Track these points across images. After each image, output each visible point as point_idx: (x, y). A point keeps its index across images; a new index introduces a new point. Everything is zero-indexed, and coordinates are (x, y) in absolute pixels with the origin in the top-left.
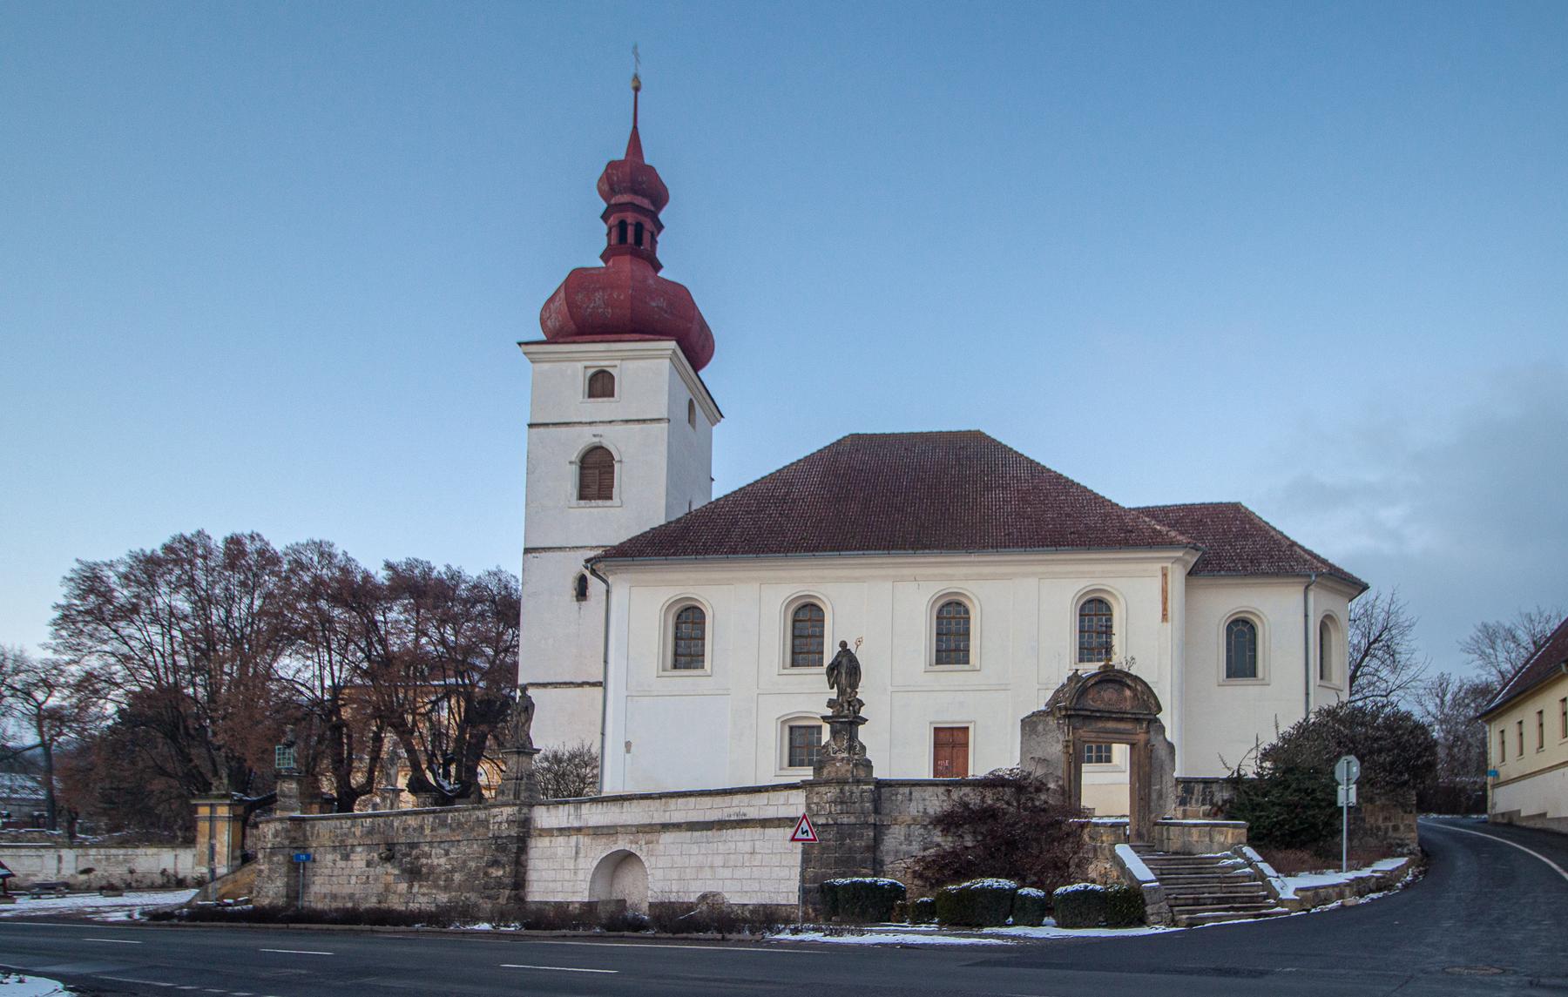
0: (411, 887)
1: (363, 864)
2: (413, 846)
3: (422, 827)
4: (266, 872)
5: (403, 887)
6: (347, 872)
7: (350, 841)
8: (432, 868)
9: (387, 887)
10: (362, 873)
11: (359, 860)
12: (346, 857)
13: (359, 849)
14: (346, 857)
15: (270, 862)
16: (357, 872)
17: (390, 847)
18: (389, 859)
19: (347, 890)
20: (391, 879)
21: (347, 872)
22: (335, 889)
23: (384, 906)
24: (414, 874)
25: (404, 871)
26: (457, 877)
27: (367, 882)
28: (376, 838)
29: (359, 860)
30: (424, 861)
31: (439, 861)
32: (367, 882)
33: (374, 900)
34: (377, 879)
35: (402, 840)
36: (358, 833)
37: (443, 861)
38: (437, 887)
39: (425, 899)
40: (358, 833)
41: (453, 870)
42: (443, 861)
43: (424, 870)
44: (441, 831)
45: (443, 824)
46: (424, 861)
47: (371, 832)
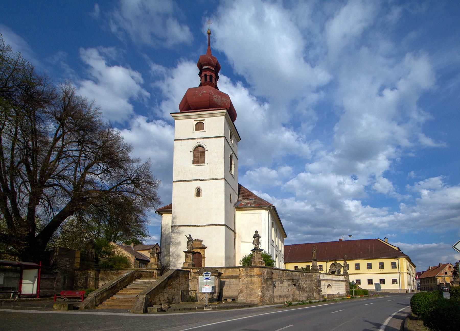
0: (299, 292)
1: (287, 285)
3: (299, 275)
5: (298, 292)
6: (283, 288)
7: (283, 278)
8: (303, 287)
10: (287, 288)
11: (286, 283)
12: (282, 283)
13: (285, 281)
14: (282, 283)
15: (267, 283)
17: (293, 280)
19: (284, 294)
22: (280, 294)
24: (300, 288)
27: (288, 291)
28: (289, 278)
29: (286, 283)
31: (303, 285)
32: (288, 291)
33: (292, 296)
34: (291, 290)
36: (285, 275)
37: (304, 285)
39: (303, 295)
40: (285, 275)
42: (304, 285)
44: (304, 277)
47: (288, 275)
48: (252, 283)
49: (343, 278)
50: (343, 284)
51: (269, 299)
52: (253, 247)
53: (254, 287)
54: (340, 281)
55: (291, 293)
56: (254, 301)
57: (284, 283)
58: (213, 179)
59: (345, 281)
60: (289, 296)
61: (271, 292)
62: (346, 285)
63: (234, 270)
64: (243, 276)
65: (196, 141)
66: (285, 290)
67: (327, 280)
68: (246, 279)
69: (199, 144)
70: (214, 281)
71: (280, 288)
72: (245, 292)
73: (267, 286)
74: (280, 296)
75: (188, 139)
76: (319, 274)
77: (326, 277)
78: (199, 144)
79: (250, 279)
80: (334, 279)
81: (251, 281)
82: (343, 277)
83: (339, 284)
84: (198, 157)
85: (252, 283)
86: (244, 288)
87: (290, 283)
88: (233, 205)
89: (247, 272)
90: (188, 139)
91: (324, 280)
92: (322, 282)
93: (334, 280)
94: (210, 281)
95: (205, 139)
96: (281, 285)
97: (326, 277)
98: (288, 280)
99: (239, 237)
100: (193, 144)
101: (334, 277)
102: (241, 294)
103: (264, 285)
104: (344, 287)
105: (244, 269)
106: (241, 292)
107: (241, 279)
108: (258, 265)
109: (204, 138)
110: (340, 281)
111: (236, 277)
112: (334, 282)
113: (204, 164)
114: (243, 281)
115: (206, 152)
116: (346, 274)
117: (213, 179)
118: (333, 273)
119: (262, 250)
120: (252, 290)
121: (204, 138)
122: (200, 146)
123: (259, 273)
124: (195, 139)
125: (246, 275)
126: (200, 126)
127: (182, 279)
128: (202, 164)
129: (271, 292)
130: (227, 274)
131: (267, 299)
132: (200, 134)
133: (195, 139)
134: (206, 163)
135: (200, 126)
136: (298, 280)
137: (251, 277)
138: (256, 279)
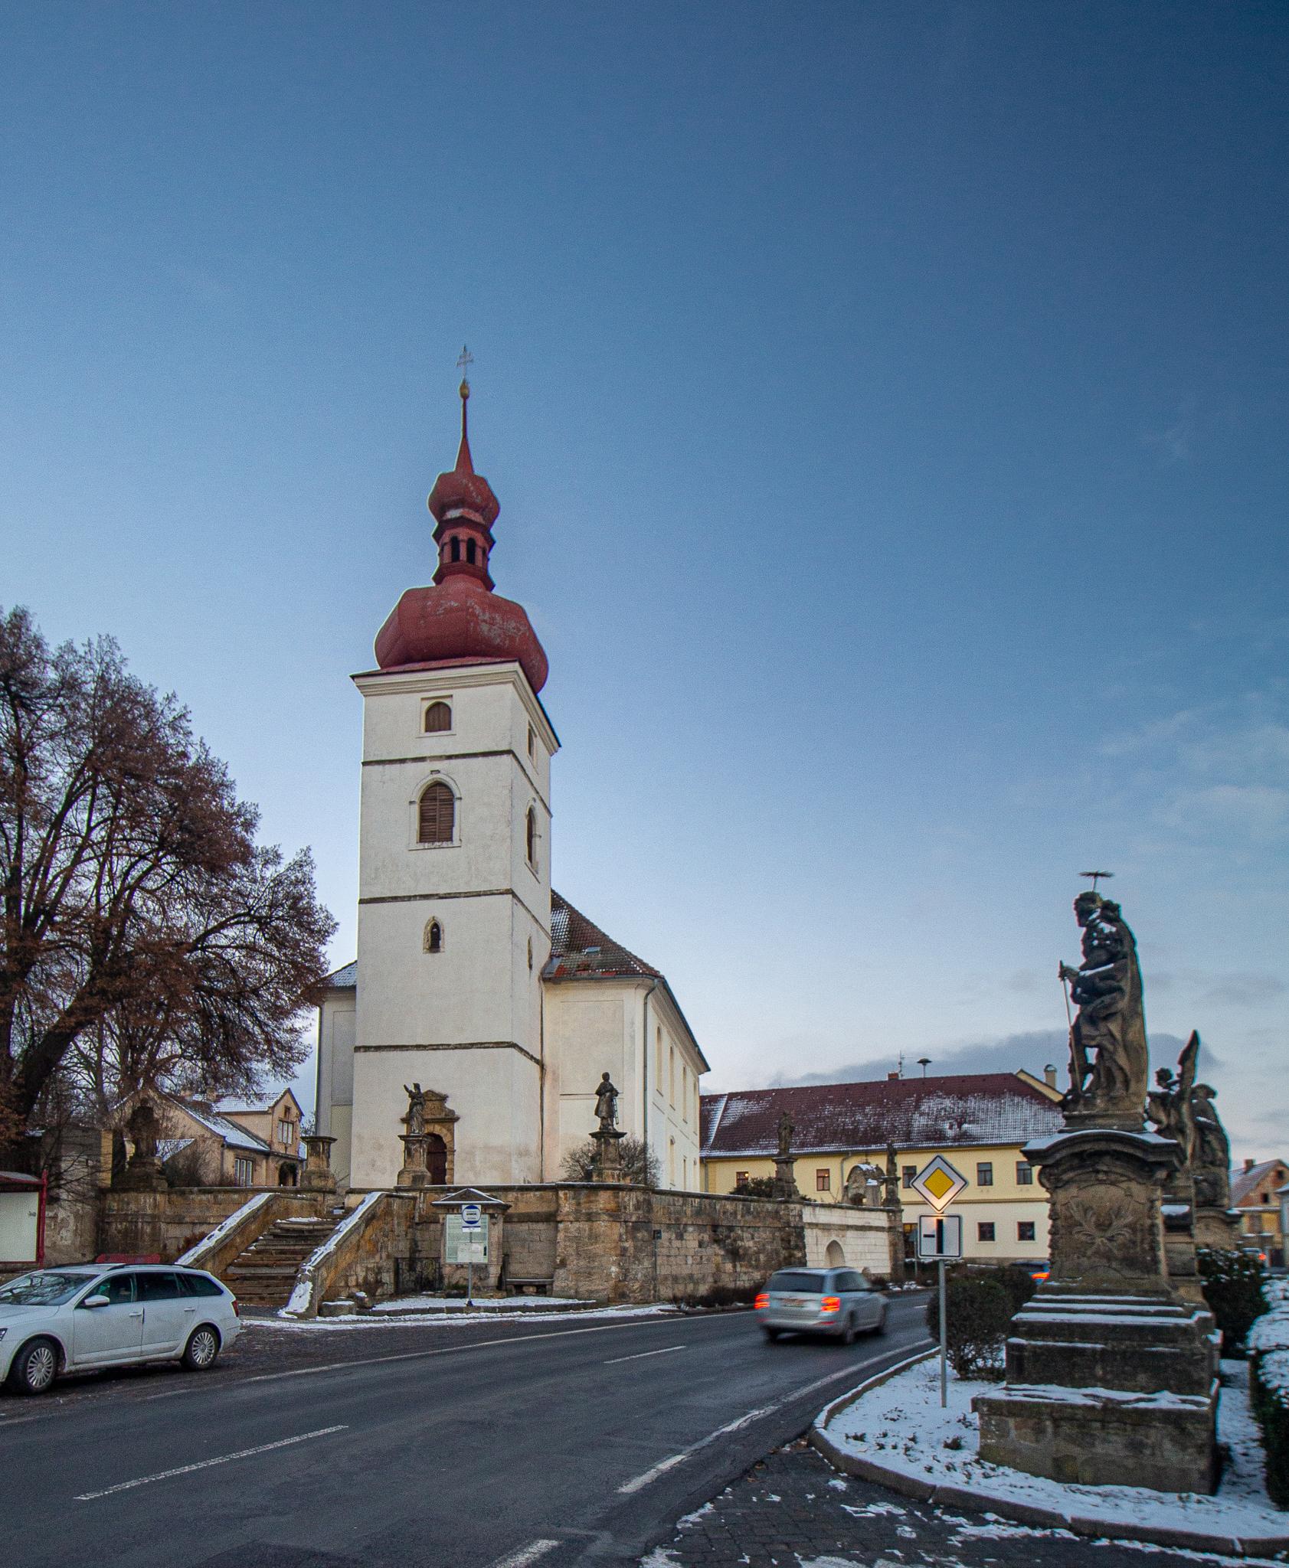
0: (735, 1267)
1: (696, 1244)
2: (731, 1229)
3: (735, 1213)
4: (632, 1250)
5: (729, 1266)
6: (683, 1252)
7: (684, 1220)
8: (746, 1249)
9: (718, 1266)
11: (691, 1239)
12: (680, 1237)
13: (690, 1229)
15: (634, 1238)
16: (692, 1252)
17: (715, 1228)
18: (716, 1241)
19: (686, 1271)
20: (719, 1259)
21: (683, 1252)
22: (675, 1271)
23: (720, 1284)
24: (735, 1254)
25: (728, 1251)
26: (762, 1257)
29: (691, 1239)
30: (739, 1243)
32: (700, 1263)
33: (711, 1279)
35: (725, 1223)
36: (689, 1212)
37: (751, 1244)
38: (751, 1266)
39: (745, 1278)
40: (689, 1212)
41: (758, 1253)
42: (751, 1244)
43: (741, 1251)
44: (749, 1218)
45: (749, 1212)
46: (739, 1243)
47: (698, 1212)
48: (594, 1237)
49: (881, 1219)
50: (883, 1238)
51: (642, 1287)
52: (596, 1125)
53: (598, 1248)
54: (870, 1228)
55: (710, 1269)
56: (597, 1291)
57: (686, 1236)
58: (478, 894)
59: (890, 1229)
60: (703, 1279)
61: (646, 1264)
62: (893, 1245)
63: (542, 1197)
64: (568, 1214)
65: (427, 766)
66: (690, 1261)
67: (826, 1227)
68: (577, 1225)
69: (436, 776)
70: (486, 1231)
71: (673, 1252)
72: (573, 1264)
73: (635, 1247)
74: (675, 1279)
75: (402, 761)
76: (798, 1206)
77: (824, 1217)
78: (436, 776)
79: (586, 1226)
80: (850, 1222)
81: (591, 1229)
82: (884, 1216)
83: (867, 1241)
84: (434, 819)
85: (594, 1237)
86: (571, 1251)
87: (706, 1237)
88: (536, 972)
89: (579, 1204)
90: (402, 761)
91: (816, 1225)
92: (808, 1232)
93: (849, 1227)
94: (478, 1230)
95: (453, 762)
96: (677, 1243)
97: (824, 1217)
98: (701, 1228)
99: (555, 1080)
100: (417, 777)
101: (854, 1217)
102: (561, 1272)
103: (626, 1245)
104: (886, 1249)
105: (570, 1194)
106: (563, 1264)
107: (561, 1226)
108: (610, 1182)
109: (450, 757)
110: (870, 1228)
111: (551, 1218)
112: (850, 1233)
113: (449, 844)
114: (566, 1230)
115: (457, 804)
116: (892, 1205)
117: (478, 894)
118: (856, 1202)
119: (622, 1135)
120: (592, 1257)
121: (450, 757)
122: (439, 785)
123: (613, 1205)
124: (422, 759)
125: (577, 1211)
126: (438, 717)
127: (399, 1224)
128: (445, 844)
129: (646, 1264)
130: (522, 1208)
131: (637, 1286)
132: (438, 743)
133: (422, 759)
134: (456, 842)
135: (438, 717)
136: (731, 1229)
137: (590, 1217)
138: (602, 1225)
